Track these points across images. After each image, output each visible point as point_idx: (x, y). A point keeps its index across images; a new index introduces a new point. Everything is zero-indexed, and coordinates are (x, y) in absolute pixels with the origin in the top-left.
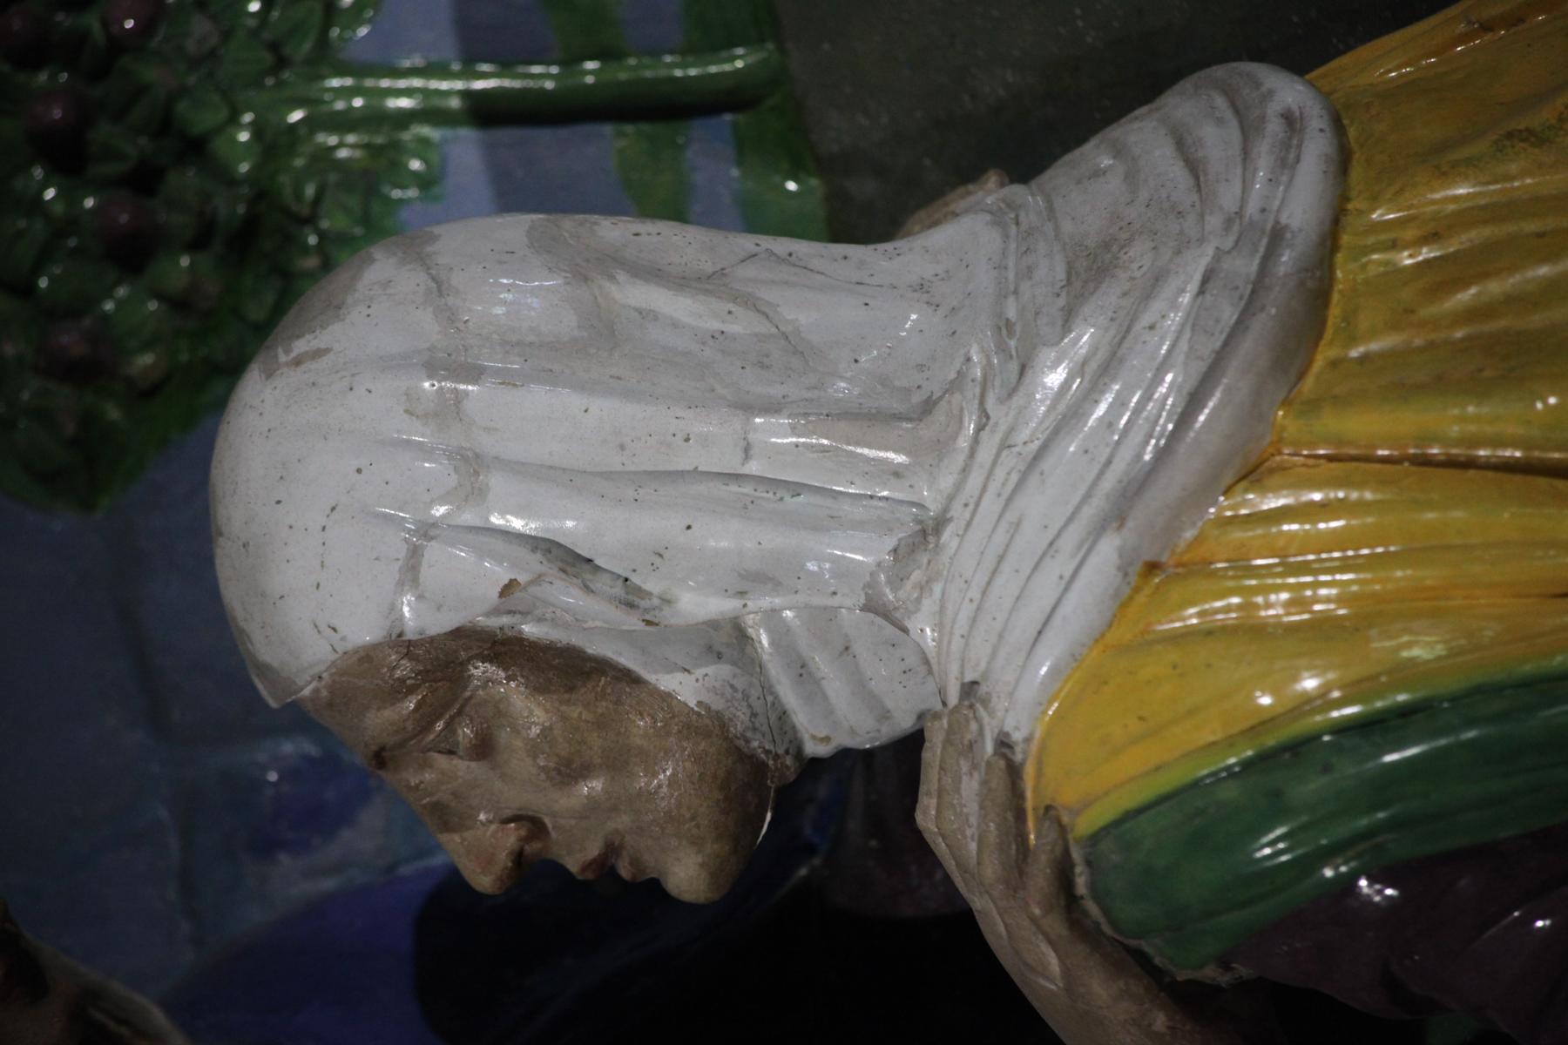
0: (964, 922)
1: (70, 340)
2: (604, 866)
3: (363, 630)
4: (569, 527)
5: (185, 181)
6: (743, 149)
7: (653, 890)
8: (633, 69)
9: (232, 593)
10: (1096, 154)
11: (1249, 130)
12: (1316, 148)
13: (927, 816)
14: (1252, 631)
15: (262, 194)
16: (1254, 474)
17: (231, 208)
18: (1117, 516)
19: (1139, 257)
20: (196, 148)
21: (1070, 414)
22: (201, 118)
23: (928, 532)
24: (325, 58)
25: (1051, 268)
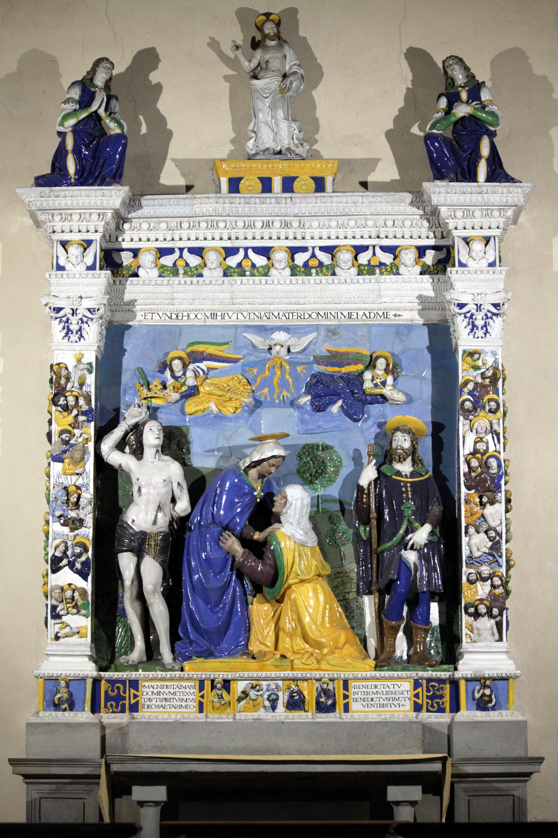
0: (270, 525)
1: (306, 472)
2: (274, 501)
3: (288, 493)
4: (293, 505)
5: (315, 478)
6: (316, 511)
7: (273, 507)
8: (320, 505)
9: (290, 485)
10: (313, 533)
11: (313, 542)
12: (312, 546)
13: (277, 524)
14: (286, 542)
15: (314, 483)
16: (294, 542)
17: (313, 481)
18: (293, 535)
19: (307, 536)
20: (317, 479)
21: (298, 532)
22: (318, 479)
23: (292, 524)
24: (321, 487)
25: (306, 531)
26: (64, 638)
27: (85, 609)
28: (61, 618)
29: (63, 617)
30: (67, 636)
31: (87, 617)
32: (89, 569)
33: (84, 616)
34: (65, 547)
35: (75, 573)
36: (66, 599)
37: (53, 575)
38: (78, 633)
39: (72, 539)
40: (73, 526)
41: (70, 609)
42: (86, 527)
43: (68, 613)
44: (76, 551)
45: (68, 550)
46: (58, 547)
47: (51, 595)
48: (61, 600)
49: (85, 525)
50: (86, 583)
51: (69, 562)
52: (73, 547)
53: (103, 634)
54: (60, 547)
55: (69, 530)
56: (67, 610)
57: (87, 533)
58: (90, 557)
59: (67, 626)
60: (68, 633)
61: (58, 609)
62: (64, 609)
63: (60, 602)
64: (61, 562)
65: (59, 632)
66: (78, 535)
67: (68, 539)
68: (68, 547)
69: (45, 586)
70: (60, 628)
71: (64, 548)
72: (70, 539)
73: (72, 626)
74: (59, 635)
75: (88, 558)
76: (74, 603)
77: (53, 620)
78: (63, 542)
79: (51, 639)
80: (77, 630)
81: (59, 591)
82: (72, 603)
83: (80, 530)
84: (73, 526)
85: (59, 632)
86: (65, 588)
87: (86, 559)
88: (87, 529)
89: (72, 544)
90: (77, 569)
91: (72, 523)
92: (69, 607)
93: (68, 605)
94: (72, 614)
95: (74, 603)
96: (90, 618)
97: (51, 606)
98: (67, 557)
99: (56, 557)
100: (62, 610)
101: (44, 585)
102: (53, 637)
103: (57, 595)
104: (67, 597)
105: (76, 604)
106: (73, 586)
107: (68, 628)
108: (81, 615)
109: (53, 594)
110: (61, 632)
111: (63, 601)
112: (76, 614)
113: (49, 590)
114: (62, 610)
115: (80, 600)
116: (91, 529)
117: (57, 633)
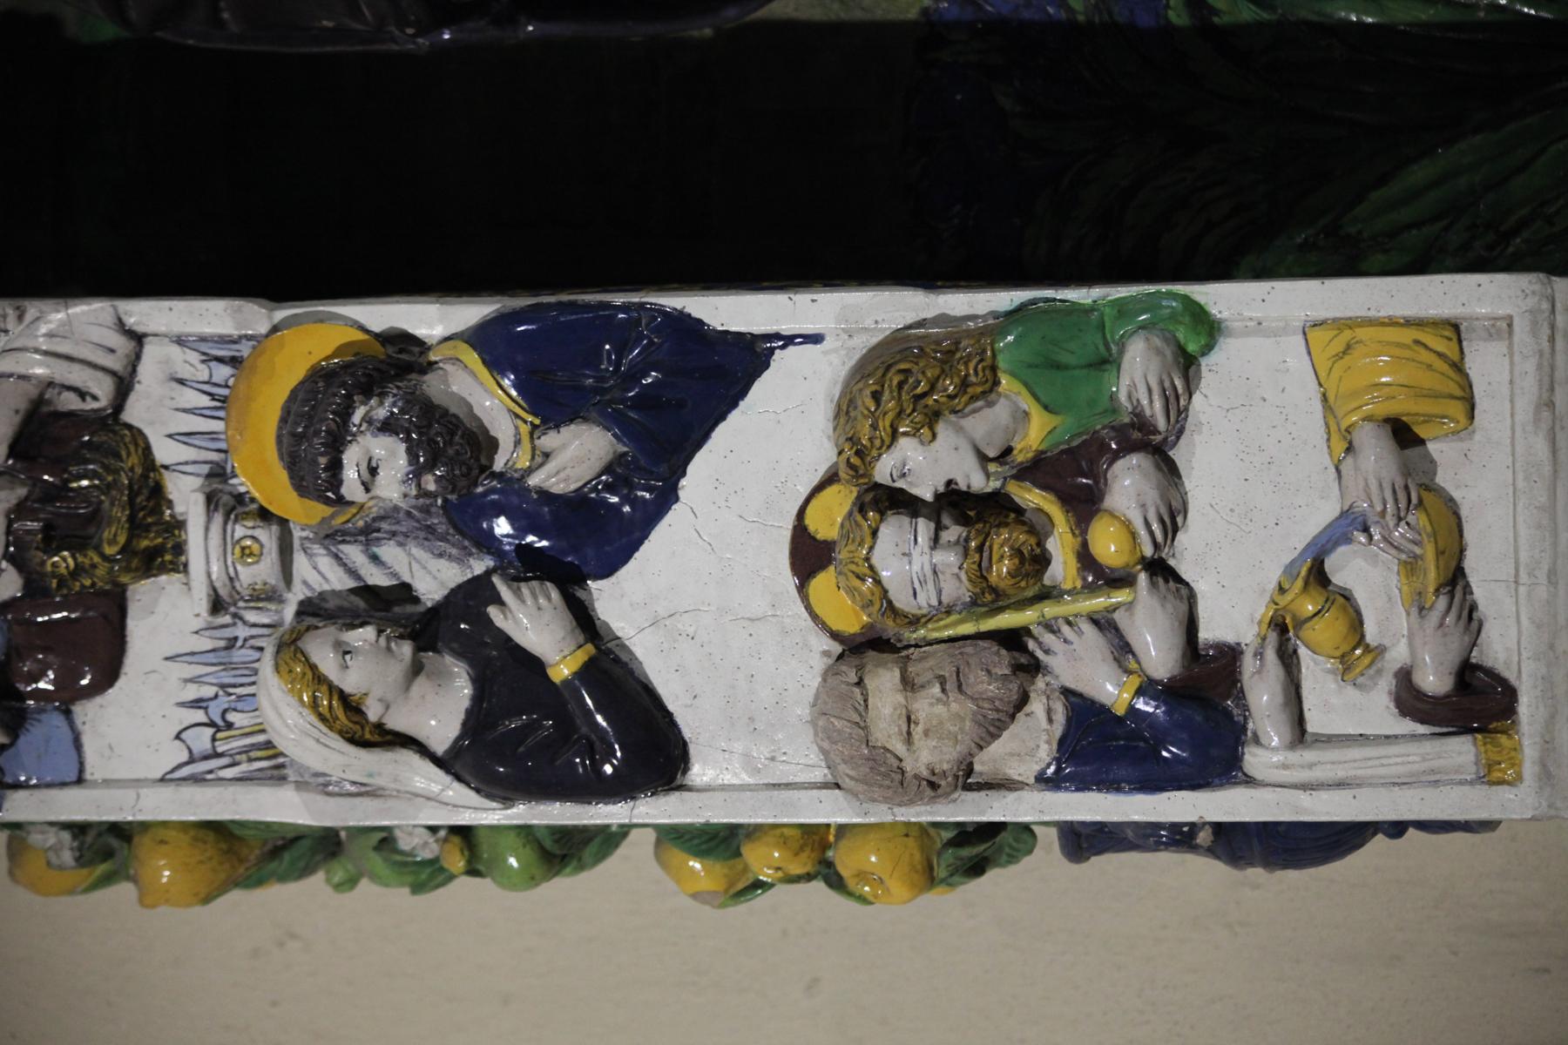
26: (1470, 617)
27: (1107, 362)
28: (1230, 655)
29: (1210, 632)
30: (1455, 580)
31: (1209, 328)
32: (624, 331)
33: (1188, 364)
34: (353, 620)
35: (667, 497)
36: (988, 598)
37: (699, 773)
38: (1403, 434)
39: (267, 537)
40: (113, 538)
41: (1109, 546)
42: (124, 385)
43: (1160, 569)
44: (392, 487)
45: (404, 592)
46: (351, 705)
47: (933, 785)
48: (1001, 660)
49: (102, 390)
50: (783, 360)
51: (528, 566)
52: (368, 535)
53: (1419, 173)
54: (351, 681)
55: (167, 582)
56: (1118, 580)
57: (189, 363)
58: (470, 313)
59: (1318, 576)
60: (1411, 566)
61: (1113, 691)
62: (1104, 623)
63: (1033, 668)
64: (533, 665)
65: (1405, 677)
66: (218, 473)
67: (266, 596)
68: (367, 591)
69: (846, 860)
70: (1346, 667)
71: (363, 636)
72: (263, 571)
73: (1324, 512)
74: (1434, 680)
75: (480, 338)
76: (1031, 497)
77: (1255, 760)
78: (290, 647)
79: (1489, 776)
80: (1376, 456)
81: (884, 681)
82: (1038, 530)
83: (165, 451)
84: (113, 538)
85: (1405, 677)
86: (852, 621)
87: (496, 365)
88: (148, 370)
89: (331, 537)
90: (618, 473)
91: (78, 544)
92: (1086, 558)
93: (1062, 567)
94: (1173, 520)
95: (1031, 497)
96: (1218, 297)
97: (1082, 784)
98: (476, 595)
99: (477, 722)
100: (1122, 650)
101: (836, 882)
102: (1461, 751)
103: (928, 706)
104: (957, 588)
105: (1037, 470)
106: (828, 519)
107: (1348, 568)
108: (1177, 409)
109: (925, 756)
110: (1398, 654)
111: (1013, 640)
112: (1170, 471)
113: (881, 814)
114: (1122, 650)
115: (987, 423)
116: (145, 313)
117: (1410, 700)
